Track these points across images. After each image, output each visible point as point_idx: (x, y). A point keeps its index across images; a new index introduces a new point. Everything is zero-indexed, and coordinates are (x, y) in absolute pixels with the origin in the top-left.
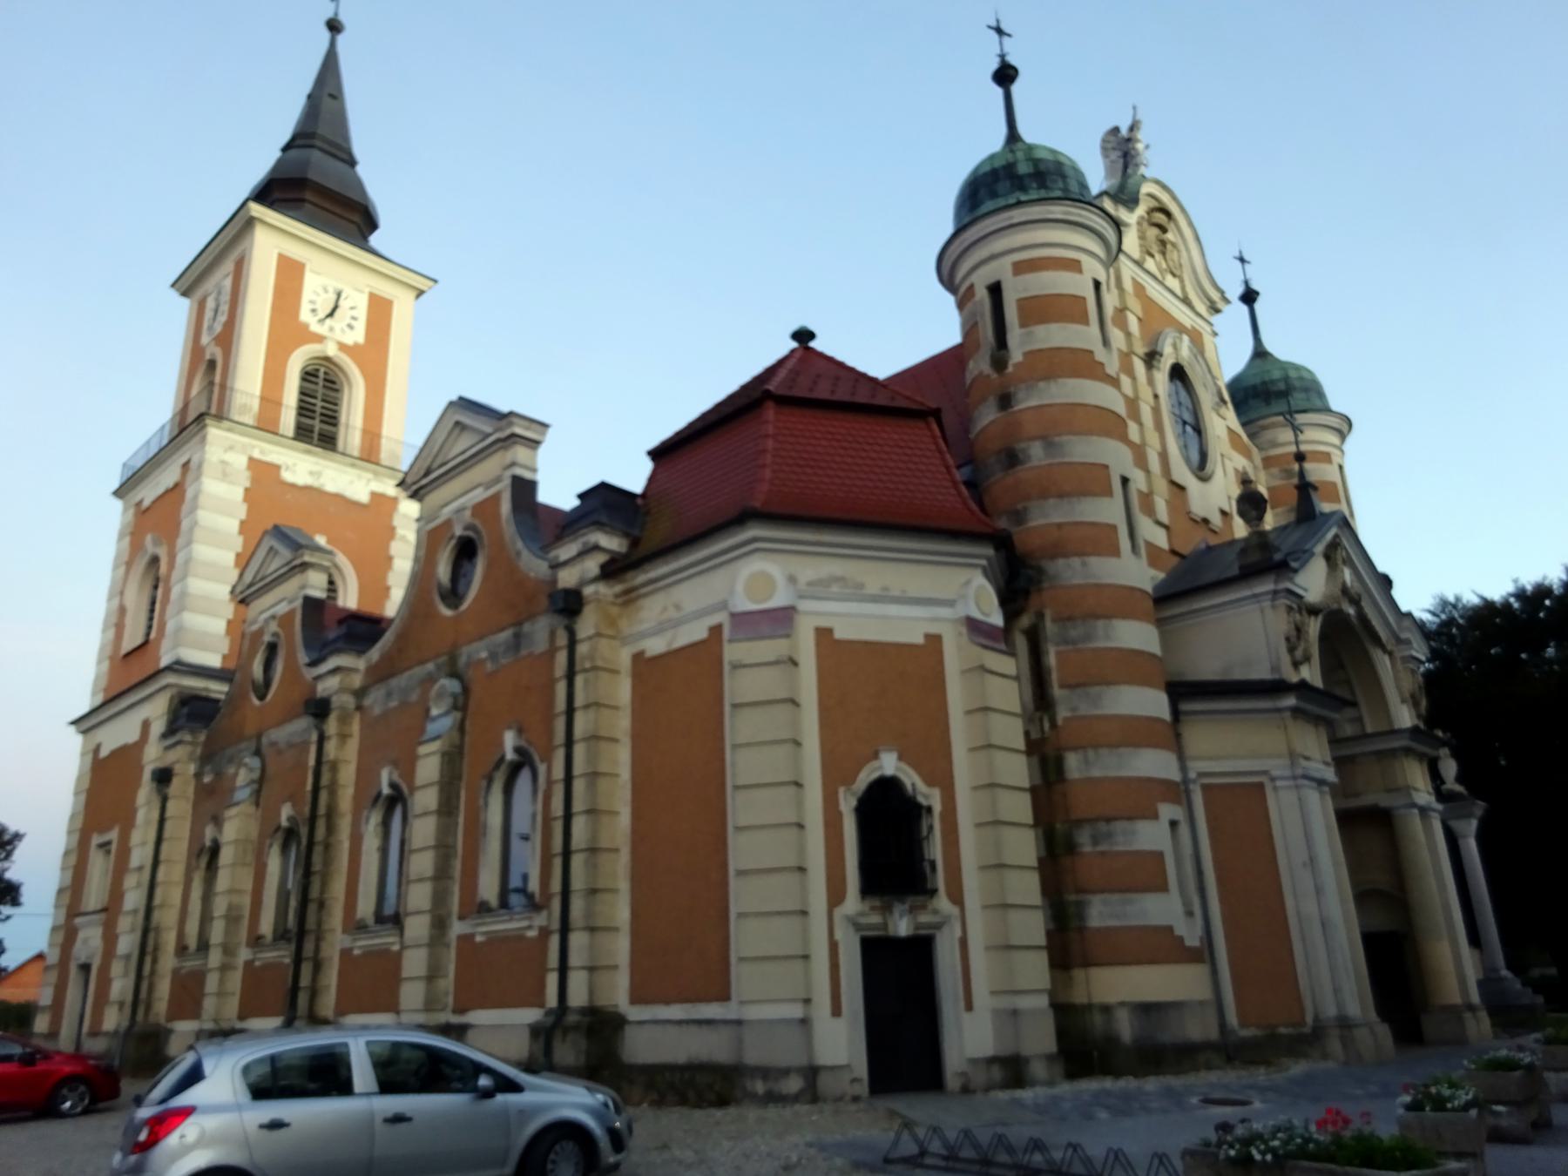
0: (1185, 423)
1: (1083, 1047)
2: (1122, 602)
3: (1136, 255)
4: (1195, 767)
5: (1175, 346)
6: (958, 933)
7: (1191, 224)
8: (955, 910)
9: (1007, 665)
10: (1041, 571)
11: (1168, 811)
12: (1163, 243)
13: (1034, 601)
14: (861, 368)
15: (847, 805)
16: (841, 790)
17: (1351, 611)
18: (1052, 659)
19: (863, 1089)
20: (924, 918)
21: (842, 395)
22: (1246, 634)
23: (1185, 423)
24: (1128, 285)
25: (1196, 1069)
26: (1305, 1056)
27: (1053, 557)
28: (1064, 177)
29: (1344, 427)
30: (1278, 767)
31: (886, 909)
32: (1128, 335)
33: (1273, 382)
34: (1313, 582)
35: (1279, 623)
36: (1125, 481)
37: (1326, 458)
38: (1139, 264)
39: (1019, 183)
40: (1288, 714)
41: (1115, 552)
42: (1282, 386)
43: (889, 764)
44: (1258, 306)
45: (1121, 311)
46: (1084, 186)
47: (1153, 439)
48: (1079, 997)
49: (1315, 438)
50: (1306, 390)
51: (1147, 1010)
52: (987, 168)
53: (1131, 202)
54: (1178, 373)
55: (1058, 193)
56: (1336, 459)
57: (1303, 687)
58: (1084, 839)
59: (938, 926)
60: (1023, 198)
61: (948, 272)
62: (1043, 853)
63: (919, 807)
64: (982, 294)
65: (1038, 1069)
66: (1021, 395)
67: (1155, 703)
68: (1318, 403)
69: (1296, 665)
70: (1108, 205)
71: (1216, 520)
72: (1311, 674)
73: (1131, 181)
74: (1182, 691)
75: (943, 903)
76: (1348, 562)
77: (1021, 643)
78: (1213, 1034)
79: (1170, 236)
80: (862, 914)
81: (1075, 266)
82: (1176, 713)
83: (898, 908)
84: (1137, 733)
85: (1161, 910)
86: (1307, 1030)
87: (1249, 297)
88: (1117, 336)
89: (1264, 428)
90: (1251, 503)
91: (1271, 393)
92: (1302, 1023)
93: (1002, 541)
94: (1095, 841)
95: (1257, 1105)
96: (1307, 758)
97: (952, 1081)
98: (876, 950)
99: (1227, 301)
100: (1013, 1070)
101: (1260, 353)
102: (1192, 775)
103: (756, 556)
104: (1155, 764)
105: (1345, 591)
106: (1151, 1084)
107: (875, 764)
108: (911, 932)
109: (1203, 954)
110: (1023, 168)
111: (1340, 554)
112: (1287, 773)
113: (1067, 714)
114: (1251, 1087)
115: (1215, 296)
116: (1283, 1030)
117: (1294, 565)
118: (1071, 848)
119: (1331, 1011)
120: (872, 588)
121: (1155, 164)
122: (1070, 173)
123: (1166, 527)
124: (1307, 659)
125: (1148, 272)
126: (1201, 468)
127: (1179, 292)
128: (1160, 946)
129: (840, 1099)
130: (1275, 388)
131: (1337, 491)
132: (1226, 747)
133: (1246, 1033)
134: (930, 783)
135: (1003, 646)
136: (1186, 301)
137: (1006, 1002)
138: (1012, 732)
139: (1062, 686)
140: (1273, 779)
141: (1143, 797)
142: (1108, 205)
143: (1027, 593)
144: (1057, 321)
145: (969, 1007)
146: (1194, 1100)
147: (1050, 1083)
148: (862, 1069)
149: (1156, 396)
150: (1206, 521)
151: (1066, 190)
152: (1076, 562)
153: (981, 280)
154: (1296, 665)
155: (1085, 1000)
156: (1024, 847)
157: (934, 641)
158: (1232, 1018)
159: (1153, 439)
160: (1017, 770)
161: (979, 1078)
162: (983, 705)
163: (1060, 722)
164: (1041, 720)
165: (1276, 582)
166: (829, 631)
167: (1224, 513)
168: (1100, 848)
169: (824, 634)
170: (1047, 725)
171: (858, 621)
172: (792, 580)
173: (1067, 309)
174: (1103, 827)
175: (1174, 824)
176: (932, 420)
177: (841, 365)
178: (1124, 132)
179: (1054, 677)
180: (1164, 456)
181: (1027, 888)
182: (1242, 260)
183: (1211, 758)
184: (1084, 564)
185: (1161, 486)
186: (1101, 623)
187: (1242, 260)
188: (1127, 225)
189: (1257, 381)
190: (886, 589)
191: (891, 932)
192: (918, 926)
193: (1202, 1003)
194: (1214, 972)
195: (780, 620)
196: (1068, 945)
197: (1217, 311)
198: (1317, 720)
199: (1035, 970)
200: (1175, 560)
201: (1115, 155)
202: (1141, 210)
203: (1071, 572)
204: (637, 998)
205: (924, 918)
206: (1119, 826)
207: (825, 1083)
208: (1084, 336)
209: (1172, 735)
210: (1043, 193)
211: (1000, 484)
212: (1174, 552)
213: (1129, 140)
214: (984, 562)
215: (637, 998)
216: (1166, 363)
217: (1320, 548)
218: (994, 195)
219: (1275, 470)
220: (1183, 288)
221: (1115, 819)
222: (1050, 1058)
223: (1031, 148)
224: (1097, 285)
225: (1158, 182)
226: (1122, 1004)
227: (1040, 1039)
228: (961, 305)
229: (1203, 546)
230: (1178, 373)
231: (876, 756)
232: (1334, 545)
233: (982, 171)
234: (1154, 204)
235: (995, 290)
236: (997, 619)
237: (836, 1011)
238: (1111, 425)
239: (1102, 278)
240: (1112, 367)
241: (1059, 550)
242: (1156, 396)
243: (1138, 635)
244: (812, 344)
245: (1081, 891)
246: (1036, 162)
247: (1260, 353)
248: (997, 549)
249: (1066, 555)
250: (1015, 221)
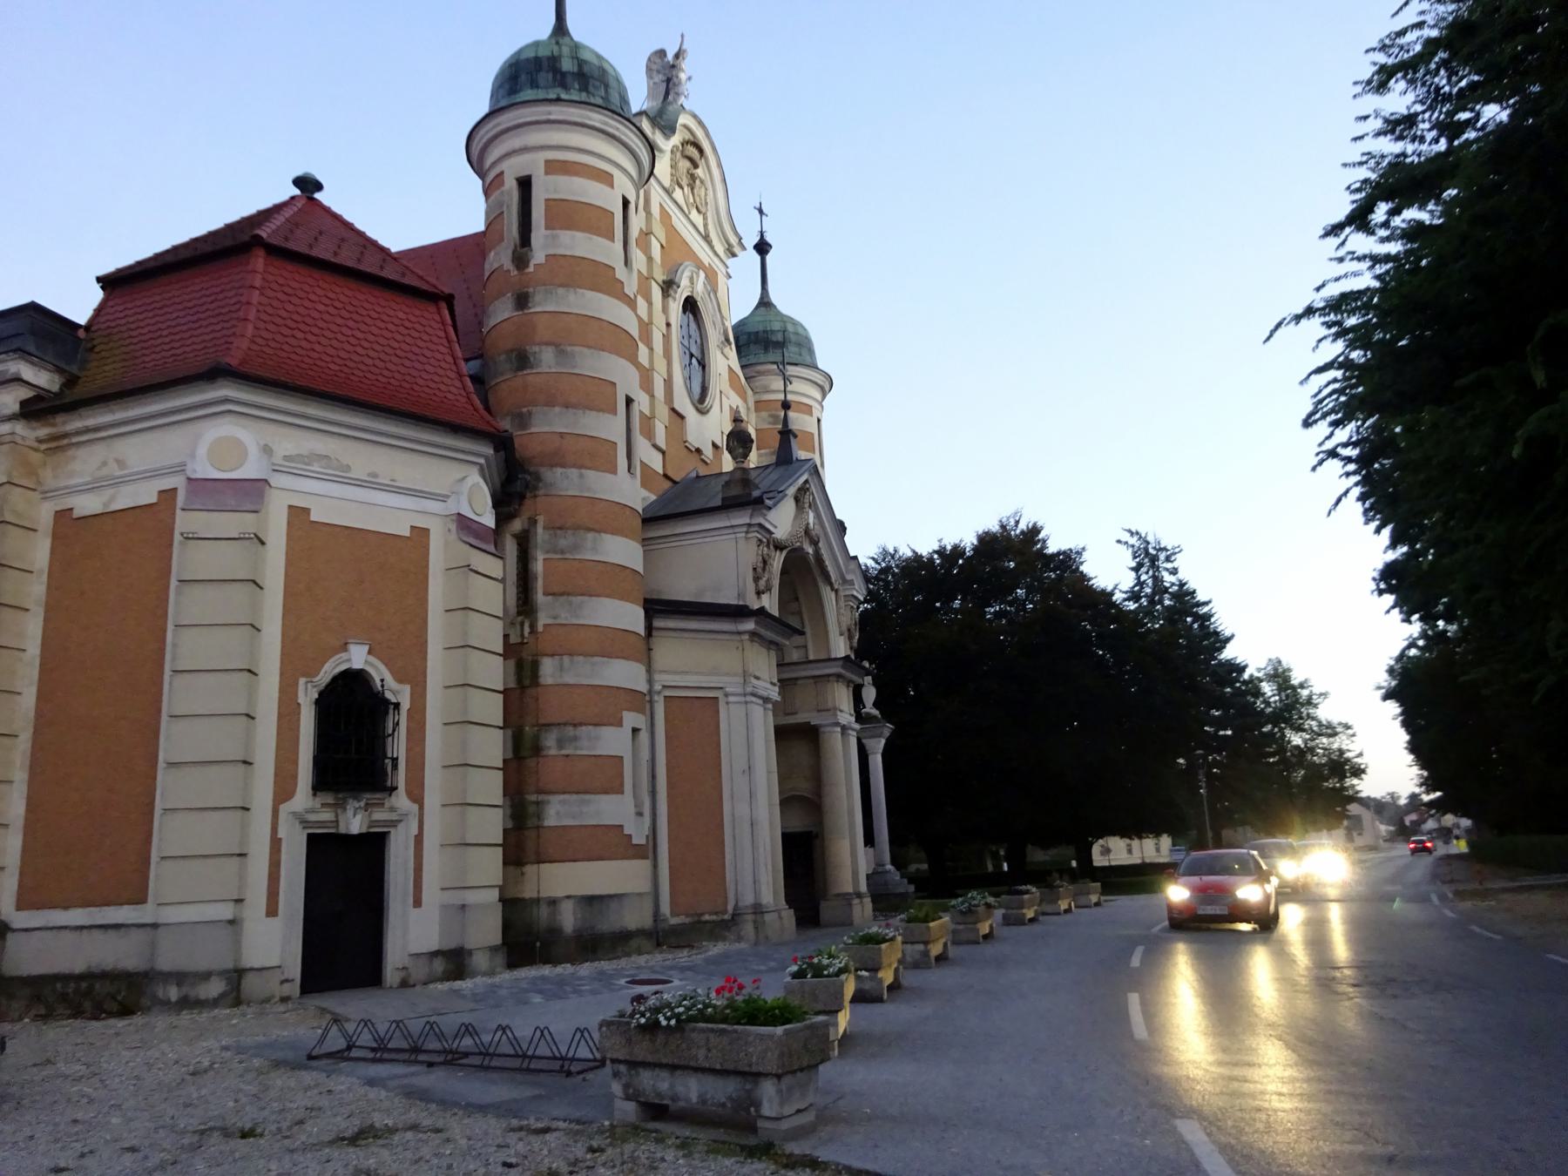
0: (692, 356)
1: (526, 939)
2: (609, 518)
3: (667, 183)
4: (661, 679)
5: (691, 279)
6: (415, 831)
7: (720, 165)
8: (415, 807)
9: (493, 566)
10: (538, 478)
11: (631, 719)
12: (693, 177)
13: (528, 508)
14: (371, 234)
15: (307, 698)
16: (302, 681)
17: (811, 551)
18: (539, 566)
19: (294, 989)
20: (379, 815)
21: (347, 258)
22: (719, 561)
23: (692, 356)
24: (655, 210)
25: (628, 955)
26: (724, 939)
27: (552, 466)
28: (607, 86)
29: (826, 385)
30: (733, 685)
31: (340, 806)
32: (650, 259)
33: (772, 332)
34: (782, 520)
35: (749, 553)
36: (629, 401)
37: (808, 410)
38: (668, 192)
39: (561, 79)
40: (746, 637)
41: (614, 471)
42: (779, 337)
43: (358, 657)
44: (769, 258)
45: (646, 234)
46: (624, 100)
47: (660, 365)
48: (528, 892)
49: (801, 390)
50: (799, 345)
51: (590, 901)
52: (532, 54)
53: (669, 129)
54: (690, 305)
55: (599, 101)
56: (816, 413)
57: (762, 611)
58: (550, 741)
59: (394, 824)
60: (563, 96)
61: (478, 151)
62: (510, 755)
63: (387, 702)
64: (510, 184)
65: (480, 961)
66: (538, 298)
67: (631, 617)
68: (808, 360)
69: (759, 593)
70: (646, 125)
71: (708, 452)
72: (770, 603)
73: (670, 108)
74: (656, 608)
75: (401, 800)
76: (813, 505)
77: (511, 547)
78: (646, 921)
79: (699, 172)
80: (312, 811)
81: (607, 179)
82: (649, 629)
83: (352, 804)
84: (611, 644)
85: (614, 810)
87: (762, 248)
88: (638, 257)
89: (760, 373)
90: (739, 440)
91: (768, 342)
92: (725, 912)
93: (503, 443)
94: (561, 743)
95: (676, 983)
96: (757, 678)
97: (391, 975)
98: (323, 848)
99: (744, 248)
100: (455, 962)
101: (765, 303)
102: (658, 687)
103: (228, 419)
104: (625, 674)
105: (807, 532)
106: (586, 969)
107: (344, 655)
108: (364, 830)
109: (647, 851)
110: (567, 65)
111: (807, 499)
112: (740, 690)
113: (550, 621)
114: (671, 968)
115: (733, 240)
116: (707, 917)
117: (768, 502)
118: (537, 750)
119: (748, 899)
120: (358, 472)
121: (696, 97)
122: (612, 83)
123: (663, 453)
124: (769, 589)
125: (676, 202)
126: (701, 401)
127: (702, 229)
128: (608, 843)
129: (267, 1000)
131: (813, 441)
132: (689, 660)
133: (674, 921)
134: (400, 681)
135: (492, 548)
136: (706, 238)
137: (456, 898)
138: (491, 634)
139: (546, 594)
140: (726, 695)
141: (610, 705)
142: (646, 125)
143: (522, 497)
144: (583, 230)
145: (418, 903)
146: (623, 982)
147: (491, 973)
148: (295, 970)
149: (668, 325)
150: (698, 451)
151: (606, 99)
152: (573, 472)
153: (512, 169)
154: (759, 593)
155: (535, 895)
156: (491, 747)
157: (421, 534)
158: (665, 909)
159: (660, 365)
160: (494, 672)
161: (420, 971)
162: (463, 606)
163: (540, 629)
164: (522, 624)
165: (751, 516)
166: (306, 511)
167: (715, 446)
168: (564, 752)
169: (298, 514)
170: (527, 630)
171: (334, 505)
172: (267, 450)
173: (592, 220)
174: (570, 731)
175: (635, 731)
176: (443, 305)
177: (349, 226)
178: (670, 57)
179: (540, 583)
180: (668, 383)
181: (491, 787)
182: (761, 211)
183: (676, 673)
184: (581, 476)
185: (663, 412)
186: (590, 535)
187: (761, 211)
188: (661, 151)
189: (761, 328)
190: (375, 476)
191: (342, 830)
192: (373, 823)
193: (640, 894)
194: (655, 866)
195: (251, 492)
196: (522, 842)
197: (734, 255)
198: (770, 644)
199: (490, 866)
200: (668, 484)
201: (658, 78)
202: (676, 140)
203: (566, 482)
204: (20, 906)
205: (379, 815)
206: (584, 730)
207: (250, 984)
208: (607, 251)
209: (643, 648)
210: (584, 96)
211: (507, 386)
212: (666, 476)
213: (673, 66)
214: (482, 461)
215: (20, 906)
216: (682, 294)
217: (792, 491)
218: (534, 85)
219: (764, 414)
220: (705, 225)
221: (581, 724)
222: (493, 949)
223: (577, 46)
224: (626, 203)
225: (695, 116)
226: (568, 897)
227: (486, 931)
228: (487, 192)
229: (694, 475)
230: (690, 305)
231: (344, 647)
232: (803, 490)
233: (524, 56)
234: (688, 136)
235: (525, 184)
236: (489, 520)
237: (272, 911)
238: (622, 343)
239: (632, 198)
240: (631, 288)
241: (557, 460)
242: (668, 325)
243: (623, 551)
244: (317, 196)
245: (540, 792)
246: (581, 63)
247: (765, 303)
248: (496, 450)
249: (563, 466)
250: (552, 117)
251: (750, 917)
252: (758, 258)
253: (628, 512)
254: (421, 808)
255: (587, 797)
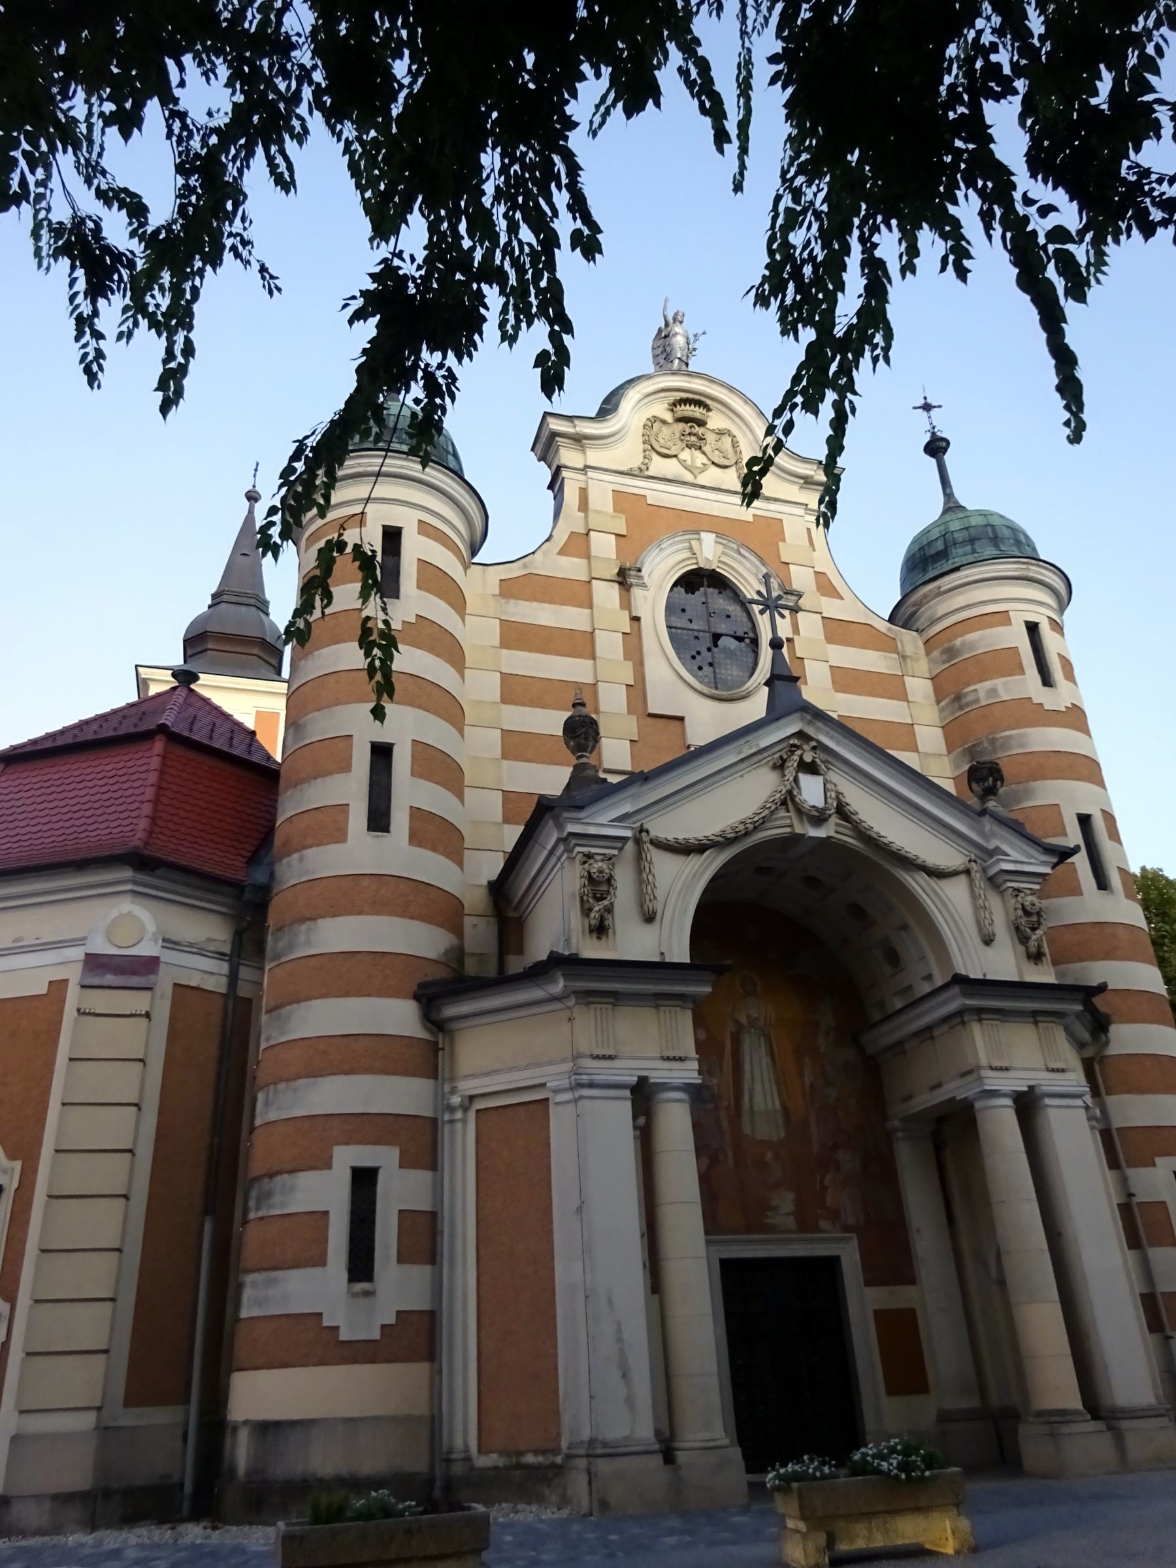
7: (747, 400)
26: (541, 1500)
40: (571, 1002)
42: (940, 546)
86: (559, 1460)
92: (556, 1451)
116: (530, 1459)
119: (586, 1434)
130: (933, 552)
133: (483, 1461)
190: (19, 939)
206: (279, 1179)
226: (246, 1422)
251: (582, 1463)
252: (933, 461)
253: (366, 882)
254: (13, 1308)
255: (274, 1274)
